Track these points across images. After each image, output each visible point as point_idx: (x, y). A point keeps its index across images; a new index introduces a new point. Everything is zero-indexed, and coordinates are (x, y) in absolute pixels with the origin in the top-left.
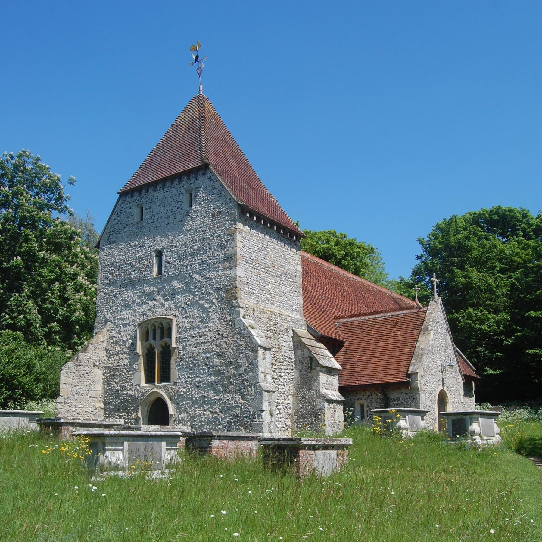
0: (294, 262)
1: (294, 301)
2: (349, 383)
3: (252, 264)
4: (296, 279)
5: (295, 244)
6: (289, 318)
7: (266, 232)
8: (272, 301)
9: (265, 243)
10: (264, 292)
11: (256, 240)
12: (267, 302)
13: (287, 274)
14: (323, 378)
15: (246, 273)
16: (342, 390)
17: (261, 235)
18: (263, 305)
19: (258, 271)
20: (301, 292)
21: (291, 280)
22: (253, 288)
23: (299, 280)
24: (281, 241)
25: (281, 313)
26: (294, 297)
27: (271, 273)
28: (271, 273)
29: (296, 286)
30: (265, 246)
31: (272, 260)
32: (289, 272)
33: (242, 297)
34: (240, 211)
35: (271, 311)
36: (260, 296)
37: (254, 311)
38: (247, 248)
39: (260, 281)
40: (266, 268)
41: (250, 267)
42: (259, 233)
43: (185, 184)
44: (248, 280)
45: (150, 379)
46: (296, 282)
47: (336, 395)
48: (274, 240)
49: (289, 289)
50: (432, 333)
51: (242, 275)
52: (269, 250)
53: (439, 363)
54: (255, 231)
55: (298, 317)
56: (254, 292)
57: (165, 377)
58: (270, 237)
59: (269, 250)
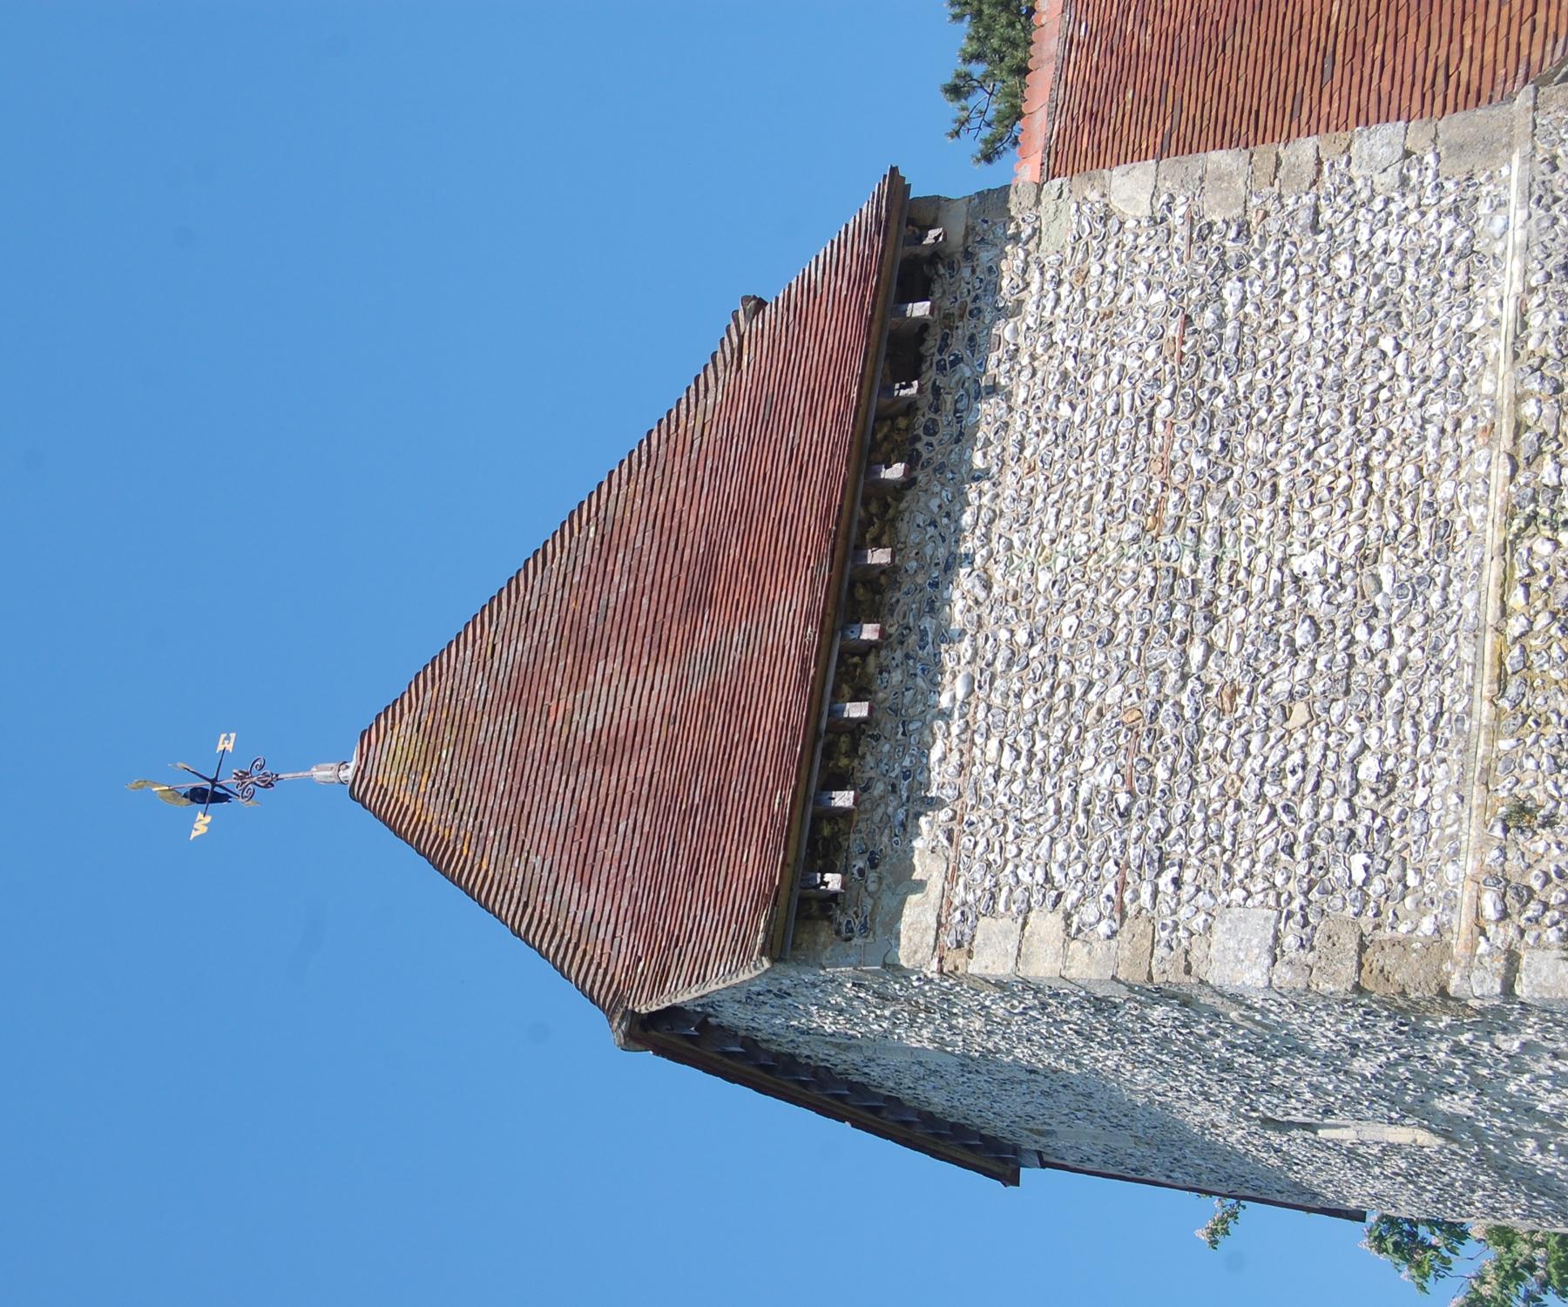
0: (1095, 270)
1: (1395, 241)
3: (1168, 792)
4: (1217, 219)
5: (968, 255)
6: (1535, 320)
7: (927, 623)
8: (1425, 543)
9: (1004, 635)
10: (1360, 633)
11: (993, 743)
12: (1435, 599)
15: (1240, 874)
17: (951, 693)
18: (1466, 653)
19: (1208, 721)
20: (1306, 148)
21: (1231, 292)
22: (1345, 776)
24: (963, 437)
25: (1506, 443)
26: (1363, 233)
27: (1207, 548)
28: (1207, 548)
29: (1273, 225)
30: (1022, 637)
31: (1110, 545)
32: (1173, 330)
33: (1427, 925)
34: (825, 934)
35: (1505, 583)
36: (1393, 694)
37: (1521, 815)
38: (1060, 848)
39: (1281, 687)
40: (1179, 613)
41: (1188, 818)
42: (944, 701)
44: (1290, 850)
46: (1244, 230)
48: (967, 519)
49: (1303, 314)
51: (1257, 923)
52: (1044, 578)
54: (935, 754)
55: (1513, 171)
56: (1369, 768)
58: (950, 565)
59: (1044, 578)
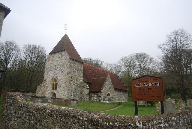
2: (91, 91)
13: (80, 70)
14: (85, 90)
16: (90, 92)
23: (83, 71)
43: (61, 53)
45: (53, 89)
47: (88, 93)
50: (107, 82)
53: (108, 88)
57: (56, 89)
